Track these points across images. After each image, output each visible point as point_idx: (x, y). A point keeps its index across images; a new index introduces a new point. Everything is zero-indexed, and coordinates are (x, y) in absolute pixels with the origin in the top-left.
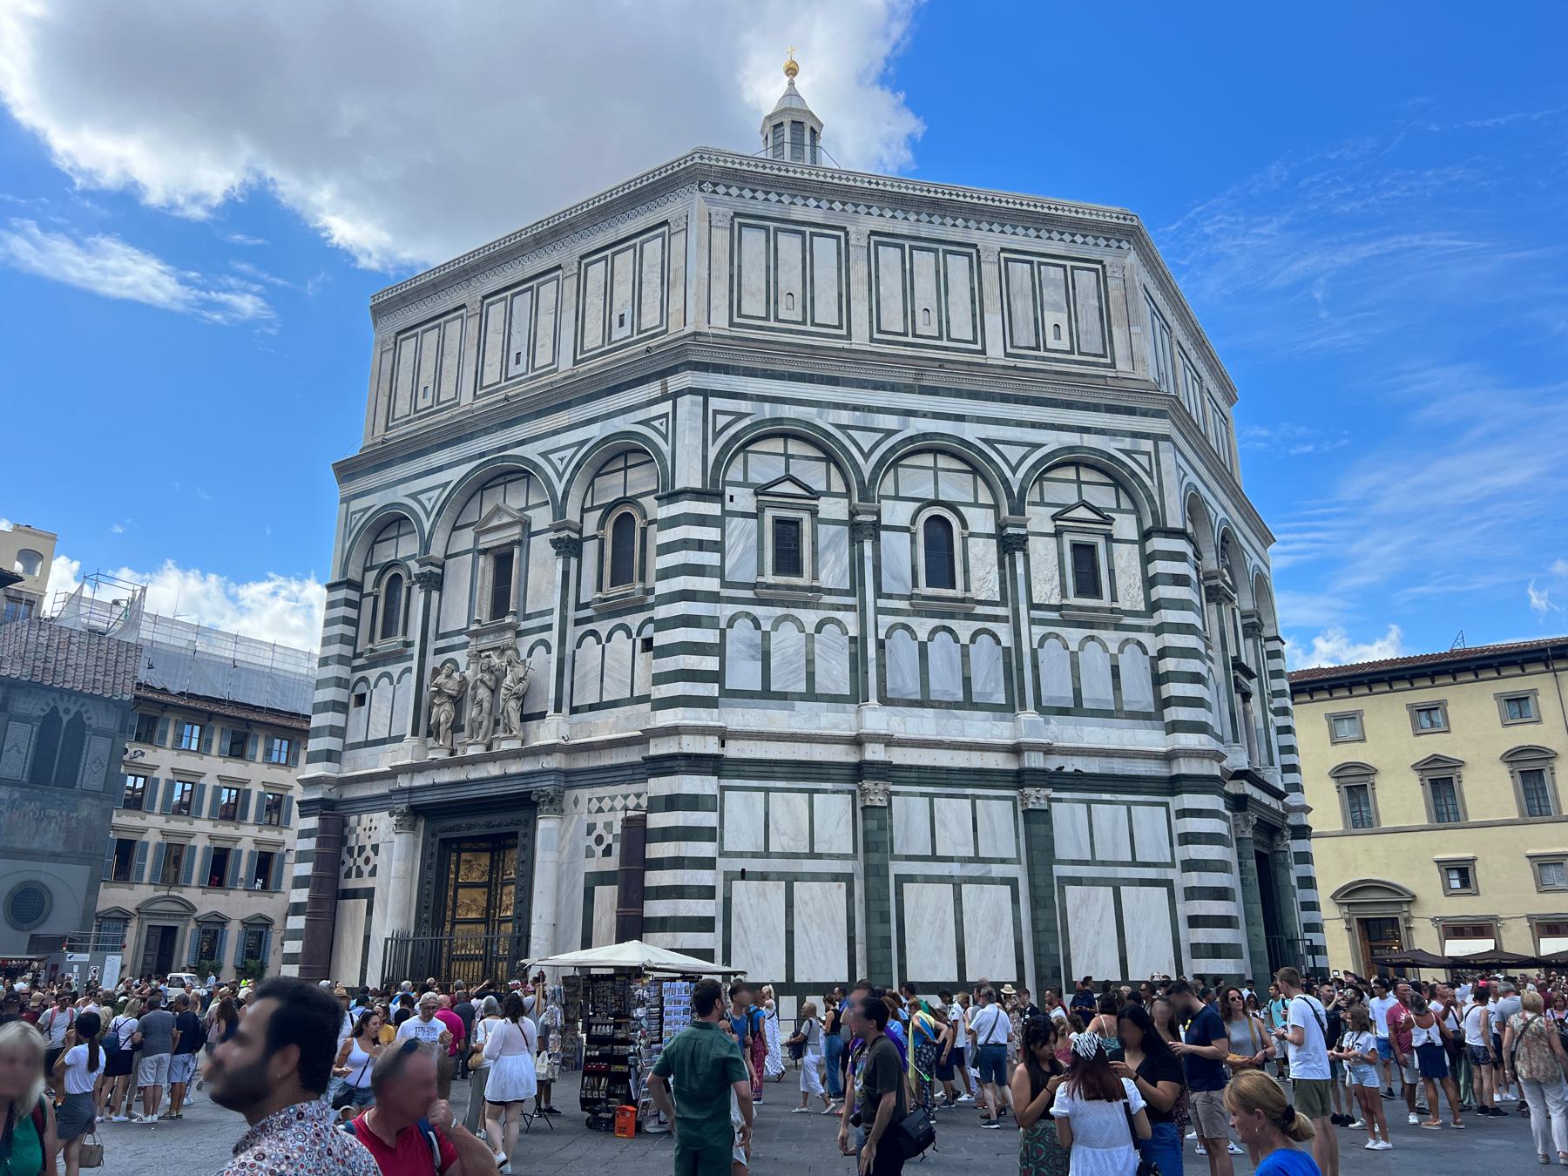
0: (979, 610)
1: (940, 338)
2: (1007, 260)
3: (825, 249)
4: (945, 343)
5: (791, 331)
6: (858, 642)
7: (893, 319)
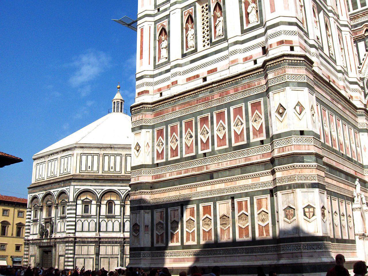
0: (116, 217)
1: (114, 171)
2: (127, 156)
3: (96, 157)
4: (115, 172)
5: (89, 173)
6: (96, 223)
7: (106, 169)
